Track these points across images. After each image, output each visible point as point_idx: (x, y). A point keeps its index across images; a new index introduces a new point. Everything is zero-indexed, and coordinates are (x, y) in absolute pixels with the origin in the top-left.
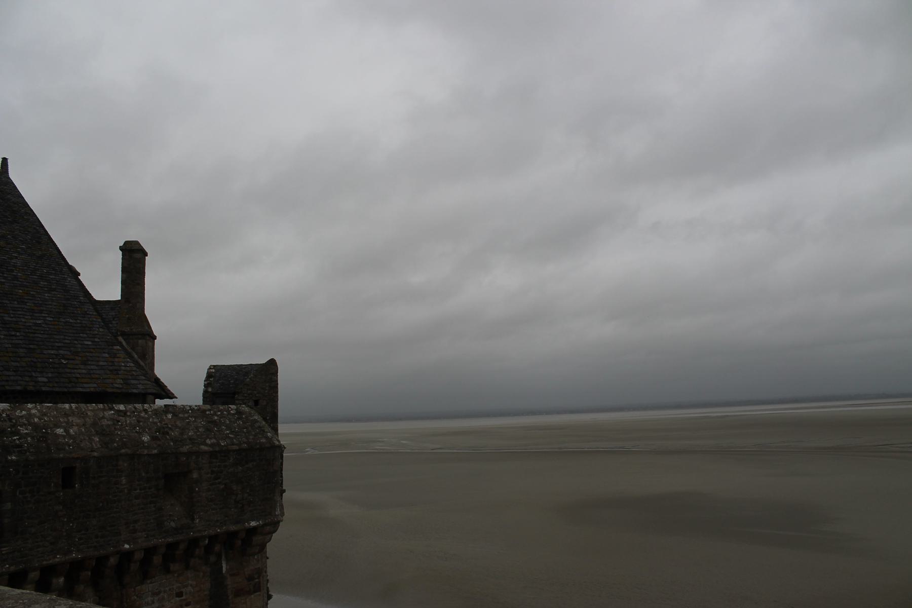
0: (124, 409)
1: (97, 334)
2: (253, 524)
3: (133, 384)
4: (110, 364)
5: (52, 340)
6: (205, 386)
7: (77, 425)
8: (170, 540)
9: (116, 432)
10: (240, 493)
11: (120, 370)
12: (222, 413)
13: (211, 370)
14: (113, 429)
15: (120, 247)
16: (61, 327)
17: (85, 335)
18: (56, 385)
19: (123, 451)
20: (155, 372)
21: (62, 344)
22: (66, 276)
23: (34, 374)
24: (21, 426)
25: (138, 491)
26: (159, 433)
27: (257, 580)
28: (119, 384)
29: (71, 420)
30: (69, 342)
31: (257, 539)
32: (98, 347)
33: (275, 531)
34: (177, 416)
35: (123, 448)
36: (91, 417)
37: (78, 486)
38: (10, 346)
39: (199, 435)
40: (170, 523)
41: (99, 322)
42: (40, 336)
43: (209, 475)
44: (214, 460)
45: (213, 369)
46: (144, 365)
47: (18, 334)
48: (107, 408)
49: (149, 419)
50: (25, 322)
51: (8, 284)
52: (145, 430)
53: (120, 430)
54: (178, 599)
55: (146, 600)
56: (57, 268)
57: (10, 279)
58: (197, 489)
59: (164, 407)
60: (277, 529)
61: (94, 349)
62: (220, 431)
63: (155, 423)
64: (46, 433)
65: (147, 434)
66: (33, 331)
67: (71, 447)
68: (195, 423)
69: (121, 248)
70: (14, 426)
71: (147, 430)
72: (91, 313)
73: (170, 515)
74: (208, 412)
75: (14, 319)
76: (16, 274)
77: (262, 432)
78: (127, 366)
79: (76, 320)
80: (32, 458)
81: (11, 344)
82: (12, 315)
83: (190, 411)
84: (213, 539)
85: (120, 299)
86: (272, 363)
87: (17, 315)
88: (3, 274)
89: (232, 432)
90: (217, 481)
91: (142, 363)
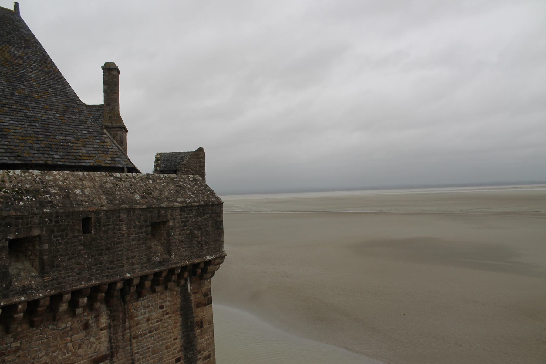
0: (120, 176)
1: (90, 127)
2: (209, 258)
3: (118, 161)
5: (61, 130)
7: (89, 188)
8: (157, 270)
9: (117, 192)
10: (200, 236)
11: (108, 151)
12: (185, 180)
13: (158, 156)
14: (114, 190)
15: (102, 67)
16: (66, 121)
17: (83, 127)
18: (66, 161)
19: (123, 206)
20: (127, 154)
22: (66, 86)
23: (51, 153)
24: (51, 187)
25: (134, 235)
26: (145, 194)
27: (210, 296)
28: (108, 161)
29: (84, 184)
30: (72, 131)
31: (210, 268)
32: (92, 135)
33: (222, 263)
34: (155, 181)
35: (123, 204)
36: (98, 182)
37: (93, 231)
38: (33, 133)
39: (171, 195)
40: (155, 258)
41: (91, 118)
42: (52, 126)
43: (180, 224)
44: (183, 213)
46: (122, 149)
47: (37, 125)
48: (108, 175)
49: (137, 183)
50: (41, 117)
51: (27, 90)
52: (136, 191)
53: (119, 191)
54: (161, 310)
55: (141, 312)
56: (60, 81)
57: (28, 86)
58: (172, 234)
59: (146, 175)
61: (89, 136)
62: (185, 192)
64: (69, 192)
65: (137, 194)
66: (47, 123)
67: (87, 203)
68: (168, 187)
69: (103, 68)
70: (45, 187)
71: (137, 191)
72: (85, 112)
73: (155, 252)
74: (175, 179)
75: (33, 114)
76: (32, 83)
77: (212, 194)
78: (113, 149)
79: (75, 116)
80: (61, 211)
81: (33, 131)
83: (164, 179)
84: (184, 268)
85: (103, 103)
86: (201, 150)
87: (35, 112)
88: (23, 83)
89: (193, 193)
90: (185, 228)
91: (120, 148)
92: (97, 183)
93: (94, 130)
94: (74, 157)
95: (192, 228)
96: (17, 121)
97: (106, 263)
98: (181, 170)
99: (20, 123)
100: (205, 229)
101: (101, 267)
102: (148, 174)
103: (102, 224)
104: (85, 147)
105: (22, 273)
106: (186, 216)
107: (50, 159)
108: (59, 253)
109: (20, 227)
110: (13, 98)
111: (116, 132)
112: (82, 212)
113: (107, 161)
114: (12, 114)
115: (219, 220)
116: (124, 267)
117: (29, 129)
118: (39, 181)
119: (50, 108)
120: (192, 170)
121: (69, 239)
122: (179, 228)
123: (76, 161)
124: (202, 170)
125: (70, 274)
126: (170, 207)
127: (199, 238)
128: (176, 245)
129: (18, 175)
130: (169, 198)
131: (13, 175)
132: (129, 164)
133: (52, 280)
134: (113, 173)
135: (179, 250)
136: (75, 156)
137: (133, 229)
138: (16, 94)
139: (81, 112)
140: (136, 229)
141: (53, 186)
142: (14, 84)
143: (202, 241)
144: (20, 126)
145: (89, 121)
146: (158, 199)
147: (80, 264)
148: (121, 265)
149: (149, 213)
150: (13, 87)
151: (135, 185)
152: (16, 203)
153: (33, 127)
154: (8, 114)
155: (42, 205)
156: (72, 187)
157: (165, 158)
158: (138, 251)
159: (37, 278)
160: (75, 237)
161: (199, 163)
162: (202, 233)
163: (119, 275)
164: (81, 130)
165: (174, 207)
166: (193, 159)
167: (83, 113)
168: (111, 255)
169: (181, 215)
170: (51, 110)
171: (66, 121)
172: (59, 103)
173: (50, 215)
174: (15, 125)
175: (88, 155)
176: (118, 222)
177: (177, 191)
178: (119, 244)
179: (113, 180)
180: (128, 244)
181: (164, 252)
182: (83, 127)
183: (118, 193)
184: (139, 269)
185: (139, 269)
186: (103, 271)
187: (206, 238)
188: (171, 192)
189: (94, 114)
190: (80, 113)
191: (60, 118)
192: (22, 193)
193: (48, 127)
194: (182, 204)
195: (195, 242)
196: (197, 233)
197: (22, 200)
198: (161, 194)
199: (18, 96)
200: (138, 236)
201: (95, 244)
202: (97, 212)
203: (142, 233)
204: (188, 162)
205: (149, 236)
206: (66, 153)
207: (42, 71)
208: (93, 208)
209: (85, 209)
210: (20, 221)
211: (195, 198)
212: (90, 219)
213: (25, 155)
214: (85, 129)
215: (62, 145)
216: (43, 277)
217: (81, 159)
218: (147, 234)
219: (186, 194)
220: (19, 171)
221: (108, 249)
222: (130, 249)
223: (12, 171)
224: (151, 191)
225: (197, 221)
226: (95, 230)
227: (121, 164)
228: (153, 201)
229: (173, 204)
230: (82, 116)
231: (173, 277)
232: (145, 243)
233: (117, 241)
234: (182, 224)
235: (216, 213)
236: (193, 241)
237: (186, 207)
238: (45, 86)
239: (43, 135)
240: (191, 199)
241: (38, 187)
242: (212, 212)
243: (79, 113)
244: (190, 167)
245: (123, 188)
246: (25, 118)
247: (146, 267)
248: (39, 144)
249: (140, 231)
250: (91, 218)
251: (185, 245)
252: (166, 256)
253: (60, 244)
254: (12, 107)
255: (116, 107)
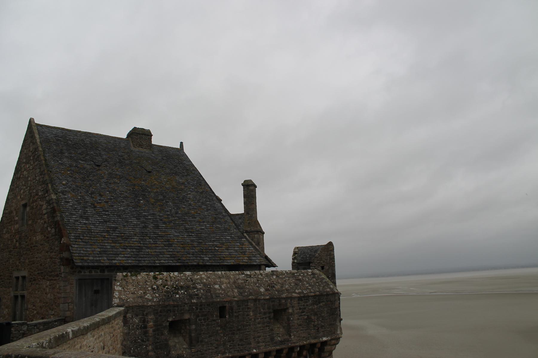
1: (233, 233)
2: (325, 339)
3: (253, 260)
4: (241, 249)
5: (210, 237)
6: (293, 259)
7: (226, 283)
8: (278, 348)
10: (316, 321)
11: (246, 252)
12: (304, 275)
13: (296, 250)
14: (244, 285)
16: (214, 230)
17: (227, 234)
18: (213, 261)
19: (250, 297)
21: (215, 239)
22: (215, 202)
23: (202, 256)
24: (197, 284)
25: (259, 320)
29: (222, 281)
31: (327, 348)
32: (234, 239)
33: (338, 344)
34: (278, 277)
35: (250, 296)
36: (233, 279)
38: (190, 241)
39: (291, 287)
40: (277, 338)
41: (233, 226)
42: (204, 235)
43: (298, 311)
44: (301, 302)
45: (296, 249)
46: (258, 248)
47: (193, 234)
48: (240, 273)
49: (263, 279)
50: (196, 228)
51: (187, 208)
53: (248, 285)
56: (210, 198)
57: (188, 205)
58: (292, 319)
59: (271, 272)
60: (339, 343)
61: (232, 241)
63: (266, 281)
64: (210, 287)
66: (200, 232)
69: (242, 184)
70: (194, 284)
72: (229, 221)
73: (278, 334)
75: (191, 227)
76: (190, 203)
77: (327, 285)
79: (221, 225)
80: (204, 301)
81: (190, 240)
82: (190, 225)
84: (302, 347)
86: (330, 244)
88: (184, 203)
89: (310, 285)
91: (258, 248)
92: (232, 279)
93: (236, 236)
94: (219, 259)
95: (309, 314)
96: (179, 233)
97: (237, 341)
98: (314, 262)
99: (181, 234)
100: (320, 315)
101: (233, 343)
102: (273, 271)
103: (234, 311)
104: (228, 250)
105: (177, 345)
106: (304, 304)
107: (201, 261)
108: (202, 332)
109: (176, 312)
110: (177, 215)
111: (254, 235)
112: (219, 302)
113: (245, 260)
114: (176, 228)
115: (334, 307)
116: (251, 344)
117: (187, 239)
118: (190, 280)
119: (203, 220)
120: (323, 262)
121: (210, 322)
122: (297, 314)
123: (220, 261)
124: (332, 261)
125: (210, 348)
126: (289, 297)
127: (316, 323)
128: (295, 328)
129: (176, 276)
130: (288, 290)
131: (173, 276)
132: (262, 262)
133: (197, 351)
134: (244, 272)
135: (297, 332)
136: (220, 257)
137: (259, 315)
138: (179, 212)
139: (225, 221)
140: (261, 315)
141: (199, 283)
142: (178, 205)
143: (318, 325)
144: (181, 236)
145: (232, 228)
146: (279, 291)
147: (217, 341)
148: (249, 343)
149: (272, 302)
150: (177, 207)
151: (261, 281)
152: (174, 296)
153: (190, 237)
154: (174, 228)
155: (191, 297)
156: (213, 284)
157: (301, 252)
158: (263, 332)
159: (187, 350)
160: (214, 320)
161: (328, 255)
162: (318, 318)
163: (247, 351)
164: (225, 236)
165: (293, 297)
166: (324, 252)
167: (228, 222)
168: (241, 335)
169: (299, 303)
170: (204, 222)
171: (214, 230)
172: (209, 216)
173: (196, 304)
174: (178, 236)
175: (230, 256)
176: (247, 310)
177: (296, 284)
178: (247, 326)
179: (244, 277)
180: (254, 326)
181: (285, 333)
182: (227, 234)
183: (247, 287)
184: (263, 347)
185: (263, 347)
186: (235, 347)
187: (322, 322)
188: (291, 285)
189: (237, 221)
190: (225, 223)
191: (210, 228)
192: (178, 289)
193: (200, 236)
194: (300, 295)
195: (312, 326)
196: (313, 318)
197: (178, 293)
198: (282, 287)
199: (180, 214)
200: (263, 320)
201: (229, 326)
202: (230, 302)
203: (266, 318)
204: (320, 255)
205: (272, 321)
206: (213, 255)
207: (197, 192)
208: (227, 299)
209: (221, 300)
210: (176, 308)
211: (312, 289)
212: (225, 307)
213: (184, 259)
214: (228, 235)
215: (211, 249)
216: (191, 349)
217: (224, 260)
218: (270, 319)
219: (303, 287)
220: (177, 273)
221: (239, 330)
222: (256, 330)
223: (172, 273)
224: (274, 284)
225: (313, 308)
226: (229, 315)
227: (255, 262)
228: (274, 292)
229: (292, 295)
230: (226, 225)
231: (293, 354)
232: (269, 326)
233: (246, 324)
234: (300, 311)
235: (331, 301)
236: (310, 325)
237: (304, 297)
238: (199, 203)
239: (197, 242)
240: (308, 291)
241: (189, 284)
242: (326, 301)
243: (224, 223)
244: (322, 259)
245: (252, 283)
246: (184, 230)
247: (269, 345)
248: (194, 249)
249: (265, 316)
250: (226, 306)
251: (303, 328)
252: (287, 337)
253: (203, 325)
254: (176, 222)
255: (254, 215)
